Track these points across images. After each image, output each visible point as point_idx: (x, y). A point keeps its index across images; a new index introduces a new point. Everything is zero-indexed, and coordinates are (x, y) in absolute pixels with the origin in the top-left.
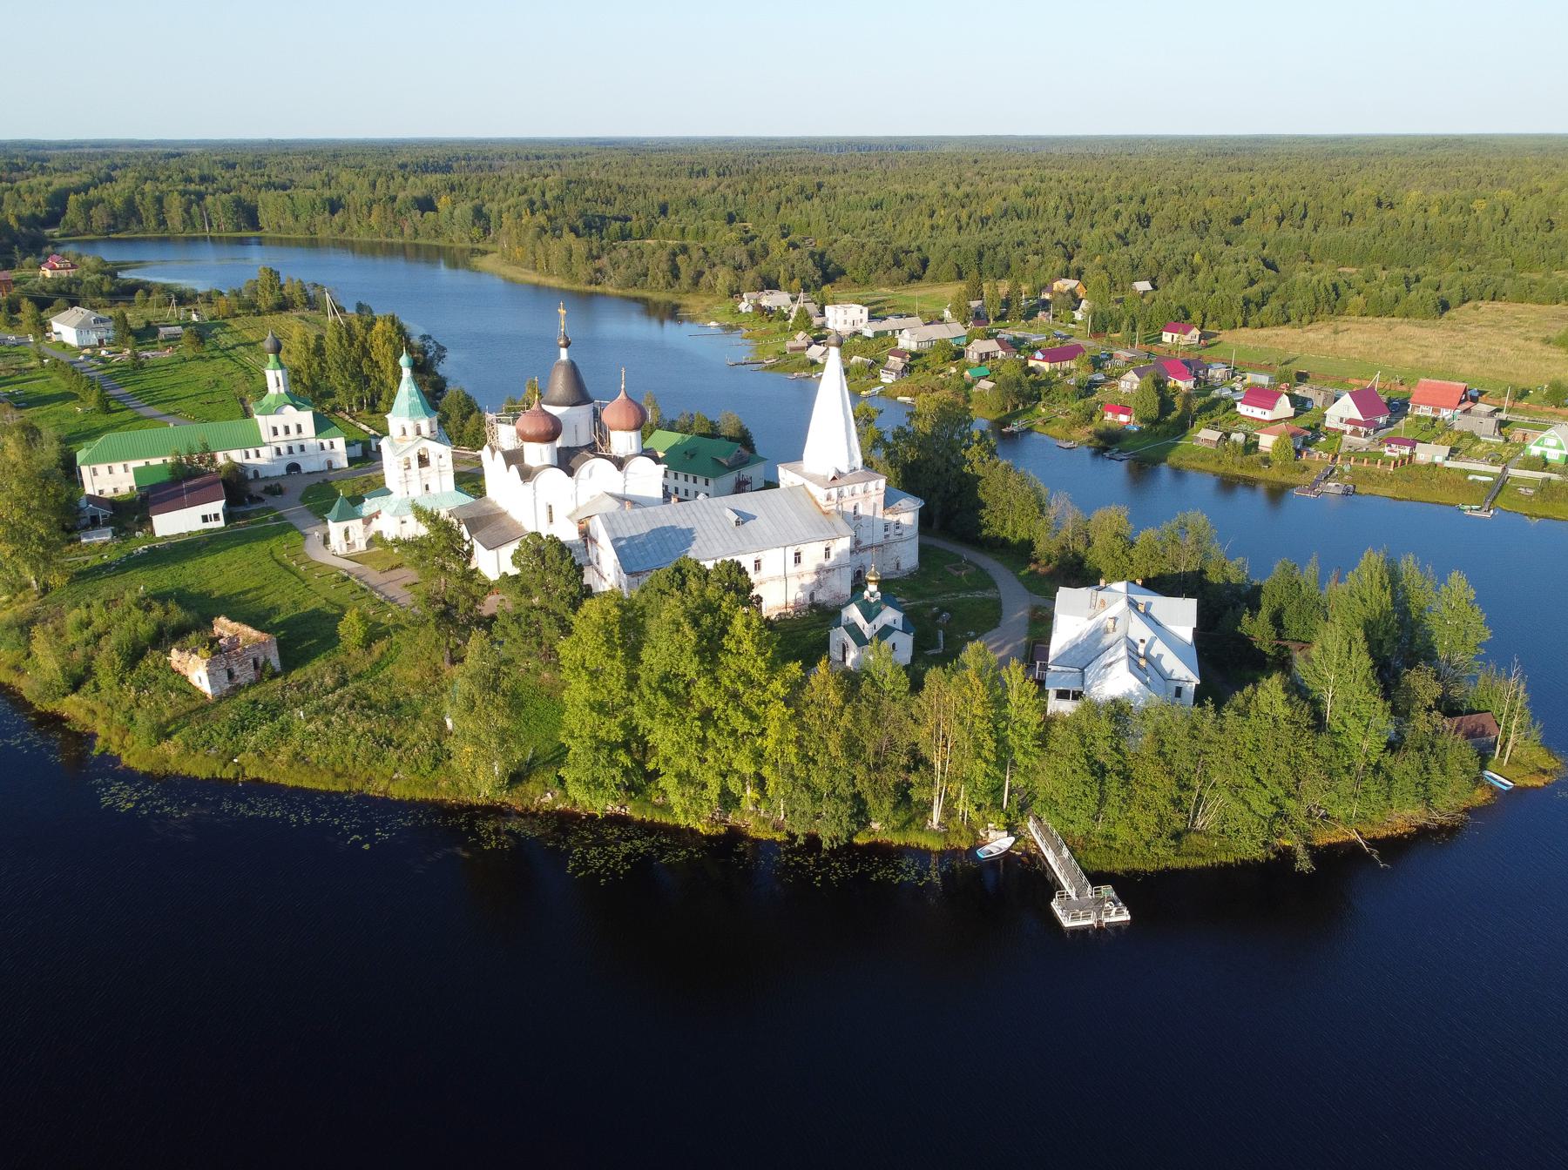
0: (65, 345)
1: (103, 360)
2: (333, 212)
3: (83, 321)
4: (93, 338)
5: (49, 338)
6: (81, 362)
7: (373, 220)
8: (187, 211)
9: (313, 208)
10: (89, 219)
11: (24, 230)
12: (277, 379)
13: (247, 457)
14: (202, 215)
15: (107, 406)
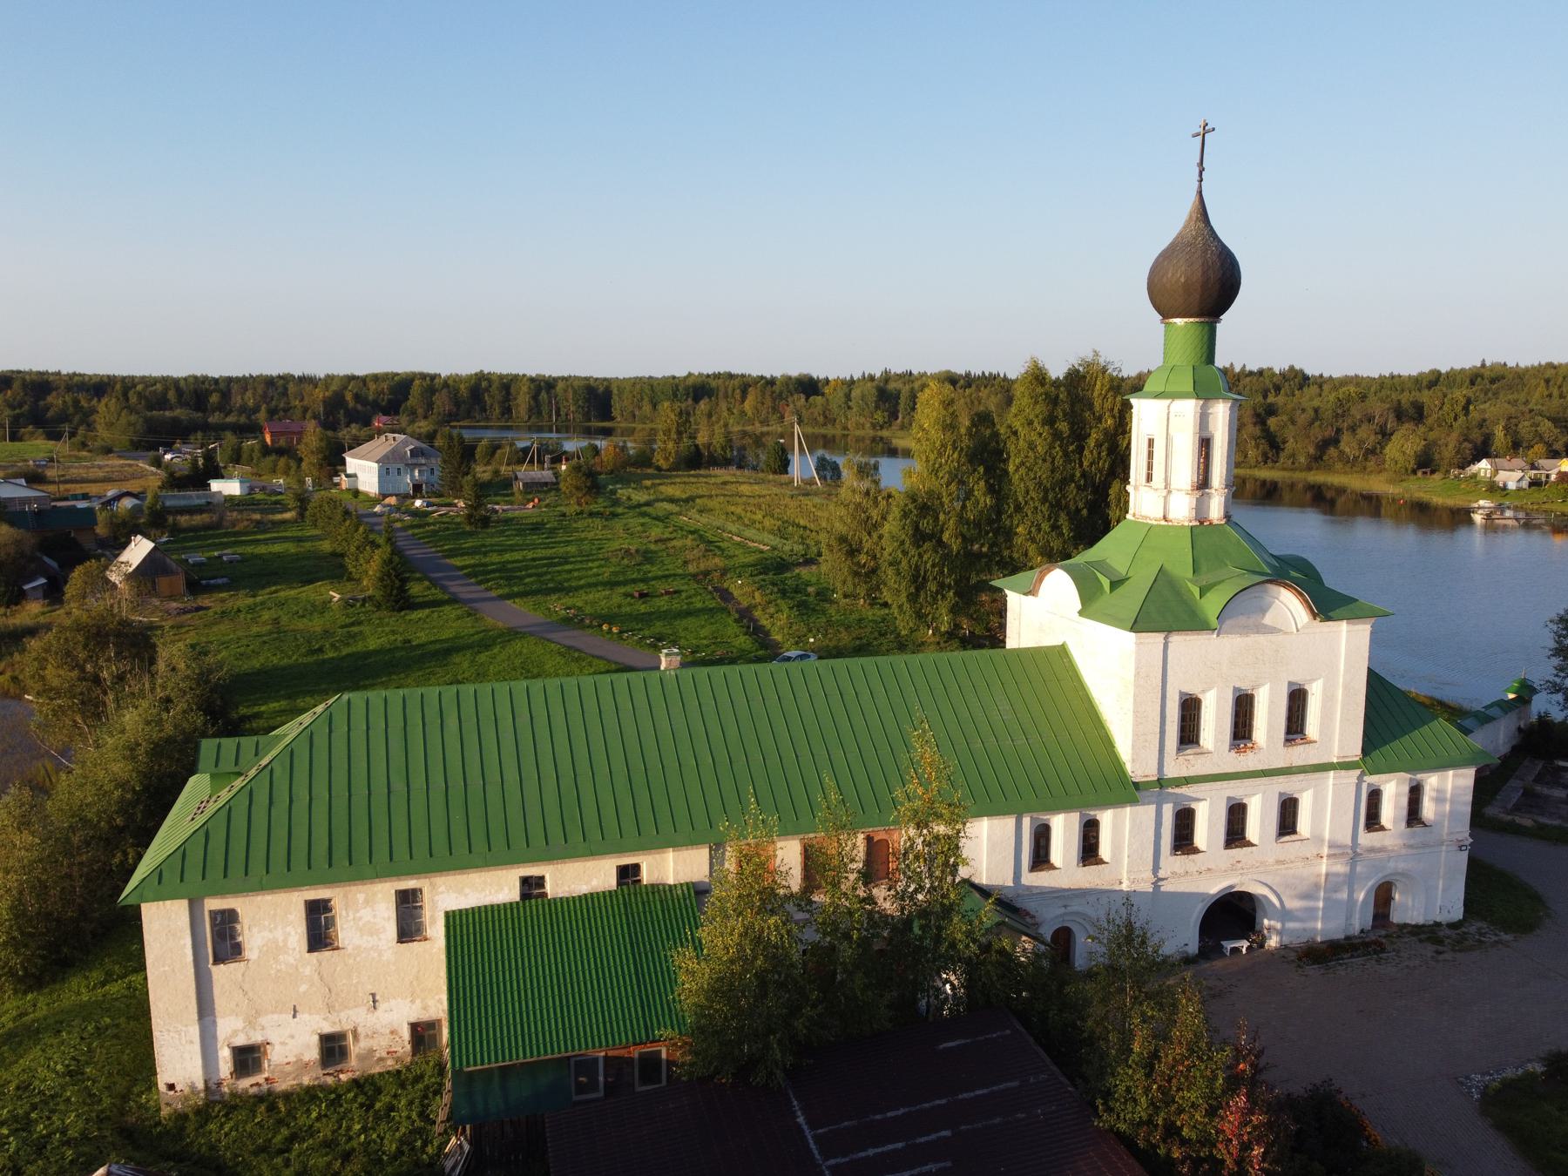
0: (356, 493)
1: (416, 513)
2: (696, 400)
3: (393, 451)
4: (407, 481)
5: (338, 484)
6: (375, 514)
7: (748, 405)
8: (535, 397)
9: (675, 395)
10: (430, 406)
11: (359, 407)
12: (1205, 444)
13: (1041, 859)
14: (550, 402)
15: (402, 590)
